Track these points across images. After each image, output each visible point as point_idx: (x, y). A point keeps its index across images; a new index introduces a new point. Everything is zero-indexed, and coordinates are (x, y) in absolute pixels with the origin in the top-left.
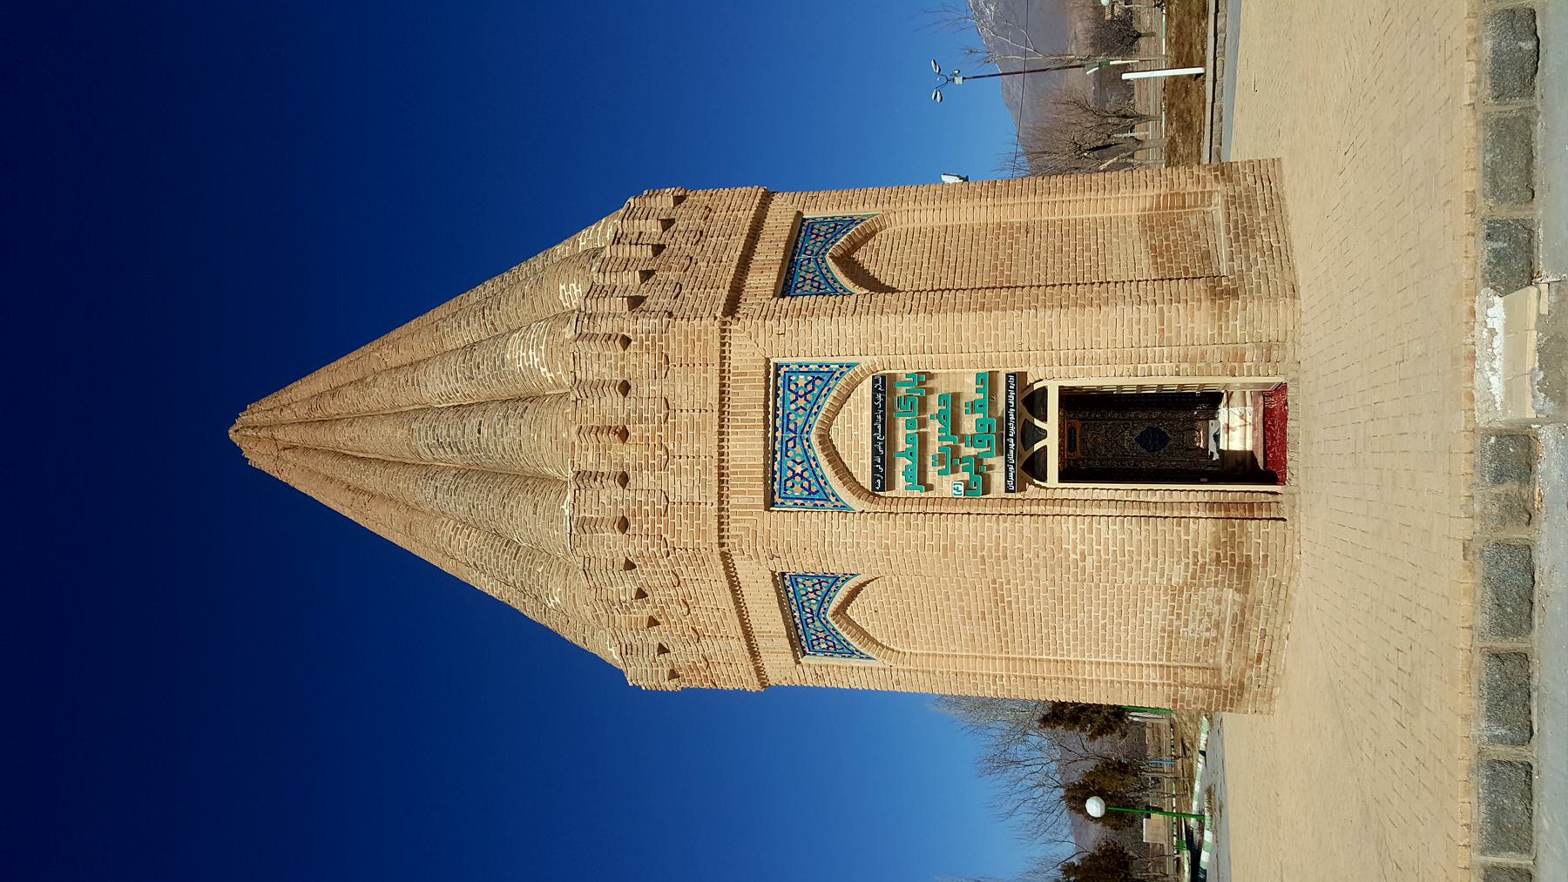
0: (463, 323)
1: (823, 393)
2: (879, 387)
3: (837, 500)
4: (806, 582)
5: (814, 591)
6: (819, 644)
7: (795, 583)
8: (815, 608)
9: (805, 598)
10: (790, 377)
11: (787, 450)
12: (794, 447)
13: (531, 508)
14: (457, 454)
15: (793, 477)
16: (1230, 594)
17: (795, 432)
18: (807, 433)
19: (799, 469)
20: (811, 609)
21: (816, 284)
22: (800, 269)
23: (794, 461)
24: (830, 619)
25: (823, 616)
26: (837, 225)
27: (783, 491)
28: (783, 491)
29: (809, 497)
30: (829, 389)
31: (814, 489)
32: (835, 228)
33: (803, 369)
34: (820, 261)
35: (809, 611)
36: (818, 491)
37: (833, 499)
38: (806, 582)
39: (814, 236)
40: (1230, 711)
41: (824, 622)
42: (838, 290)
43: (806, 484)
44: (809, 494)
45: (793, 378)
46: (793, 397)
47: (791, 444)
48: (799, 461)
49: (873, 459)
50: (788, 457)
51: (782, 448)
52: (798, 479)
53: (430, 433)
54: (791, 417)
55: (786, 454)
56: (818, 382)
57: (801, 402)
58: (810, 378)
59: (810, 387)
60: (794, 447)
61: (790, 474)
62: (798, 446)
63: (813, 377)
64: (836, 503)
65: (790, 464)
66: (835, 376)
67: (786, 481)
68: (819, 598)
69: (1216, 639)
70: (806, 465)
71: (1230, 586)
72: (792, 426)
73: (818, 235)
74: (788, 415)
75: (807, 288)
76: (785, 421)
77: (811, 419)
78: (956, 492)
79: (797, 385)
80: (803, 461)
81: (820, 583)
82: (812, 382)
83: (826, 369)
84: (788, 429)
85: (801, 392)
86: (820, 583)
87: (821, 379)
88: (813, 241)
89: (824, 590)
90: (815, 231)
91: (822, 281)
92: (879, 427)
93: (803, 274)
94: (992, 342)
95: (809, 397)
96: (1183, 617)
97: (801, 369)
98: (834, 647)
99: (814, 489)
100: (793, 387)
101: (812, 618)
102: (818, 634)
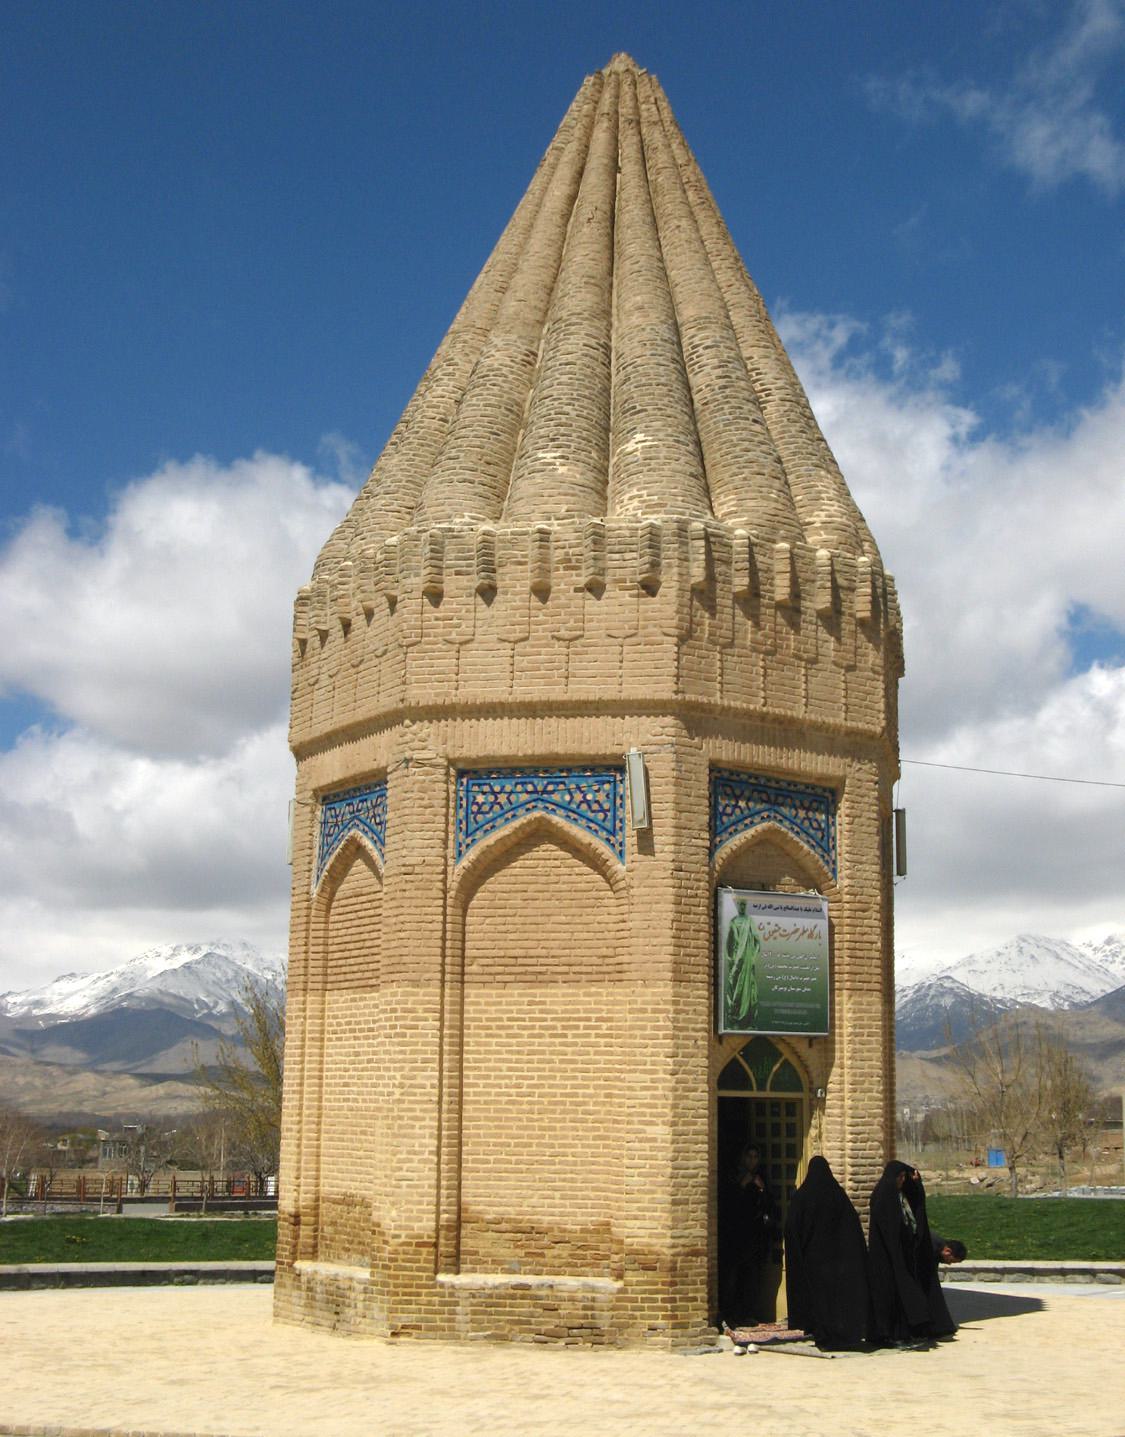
11: (760, 792)
31: (725, 819)
36: (723, 823)
45: (823, 807)
50: (753, 791)
56: (820, 835)
58: (823, 825)
59: (815, 824)
77: (787, 823)
82: (819, 828)
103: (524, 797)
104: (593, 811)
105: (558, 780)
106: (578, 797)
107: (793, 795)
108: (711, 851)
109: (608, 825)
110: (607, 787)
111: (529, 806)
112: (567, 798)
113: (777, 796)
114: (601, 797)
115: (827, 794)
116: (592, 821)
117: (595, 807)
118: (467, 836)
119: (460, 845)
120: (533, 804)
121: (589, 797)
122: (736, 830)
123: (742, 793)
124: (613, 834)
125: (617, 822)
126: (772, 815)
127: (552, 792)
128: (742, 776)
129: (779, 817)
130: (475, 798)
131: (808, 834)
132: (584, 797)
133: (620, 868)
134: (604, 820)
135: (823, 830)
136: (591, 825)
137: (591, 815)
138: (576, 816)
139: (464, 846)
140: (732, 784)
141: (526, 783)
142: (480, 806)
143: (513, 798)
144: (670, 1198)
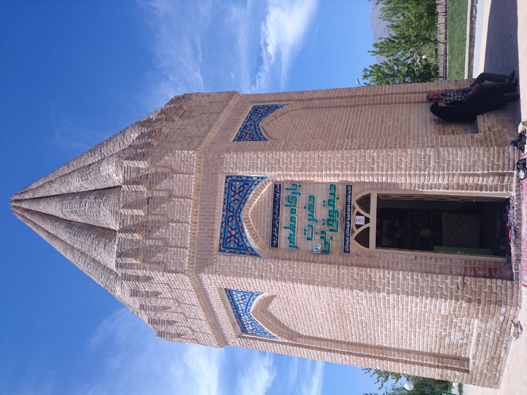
0: (93, 154)
2: (277, 190)
3: (252, 251)
4: (237, 294)
5: (242, 300)
6: (248, 327)
8: (244, 308)
9: (238, 303)
10: (232, 183)
11: (228, 222)
12: (232, 220)
13: (103, 246)
14: (78, 217)
16: (476, 322)
17: (233, 213)
18: (239, 213)
19: (233, 233)
20: (242, 309)
21: (252, 136)
22: (246, 129)
23: (231, 228)
24: (252, 315)
25: (248, 313)
26: (269, 109)
27: (225, 244)
28: (225, 244)
29: (238, 248)
30: (252, 190)
31: (240, 244)
32: (267, 110)
34: (256, 125)
35: (241, 309)
36: (242, 245)
37: (250, 250)
38: (237, 294)
39: (257, 114)
40: (474, 384)
41: (249, 316)
42: (262, 139)
43: (237, 241)
44: (238, 246)
45: (234, 184)
46: (233, 194)
47: (230, 219)
48: (234, 228)
49: (272, 229)
50: (228, 225)
51: (226, 221)
52: (233, 238)
53: (69, 206)
54: (232, 204)
56: (246, 186)
57: (237, 196)
58: (242, 184)
59: (242, 189)
60: (232, 220)
61: (229, 235)
62: (234, 221)
63: (244, 183)
64: (253, 253)
65: (229, 229)
66: (255, 183)
67: (227, 238)
68: (245, 303)
69: (466, 344)
70: (237, 231)
71: (477, 317)
72: (231, 209)
73: (258, 113)
75: (247, 138)
76: (228, 206)
78: (316, 250)
79: (235, 187)
81: (244, 295)
82: (243, 186)
84: (230, 211)
85: (237, 191)
86: (244, 295)
87: (247, 184)
88: (255, 116)
89: (247, 299)
90: (258, 112)
91: (255, 135)
92: (277, 212)
93: (246, 131)
94: (340, 167)
95: (241, 194)
96: (448, 331)
97: (238, 179)
98: (256, 329)
99: (240, 244)
100: (233, 188)
101: (243, 313)
102: (247, 322)
106: (241, 302)
107: (230, 201)
108: (254, 254)
113: (230, 211)
115: (228, 180)
123: (229, 232)
126: (238, 215)
128: (222, 232)
133: (266, 294)
135: (244, 184)
140: (226, 237)
144: (429, 298)
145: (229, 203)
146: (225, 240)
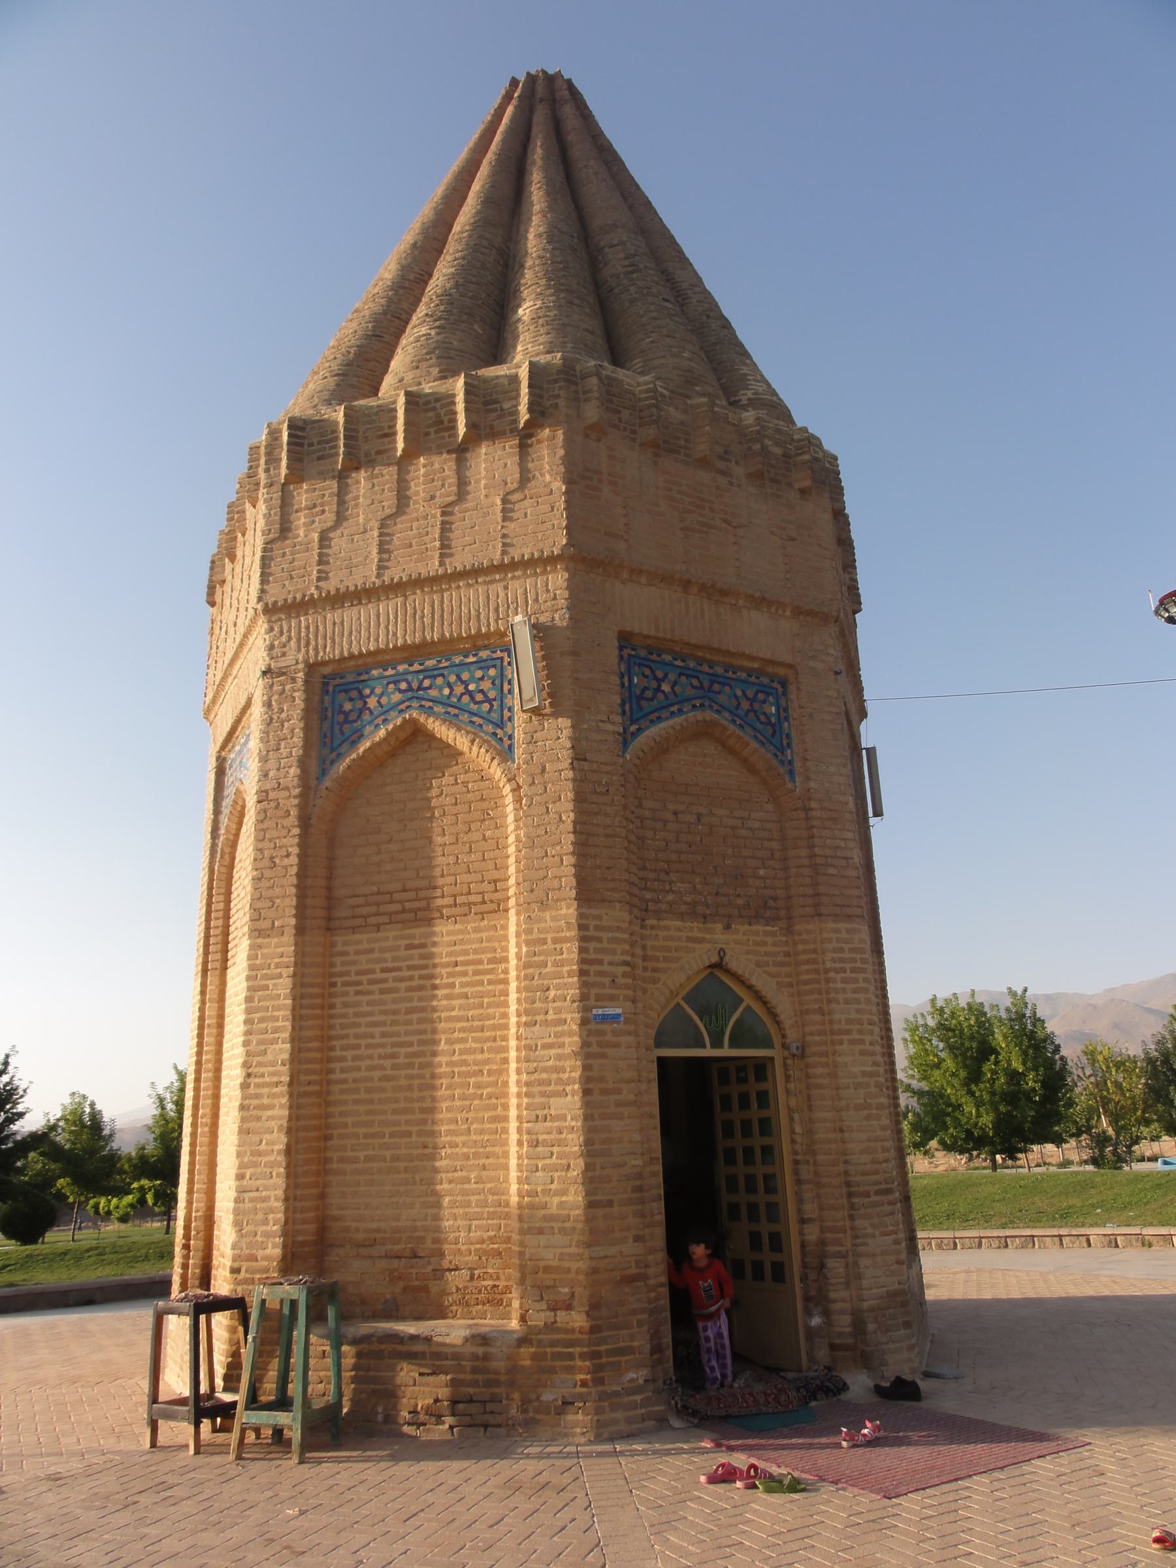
1: (758, 735)
7: (483, 665)
11: (688, 676)
12: (693, 687)
15: (656, 678)
17: (710, 690)
18: (711, 707)
19: (666, 687)
23: (675, 683)
27: (637, 661)
28: (637, 661)
31: (643, 703)
33: (784, 713)
36: (641, 709)
37: (633, 728)
43: (649, 694)
45: (771, 698)
50: (680, 675)
52: (654, 684)
54: (727, 688)
55: (683, 674)
56: (769, 730)
57: (745, 705)
58: (773, 720)
59: (763, 718)
60: (693, 687)
61: (660, 674)
62: (693, 692)
66: (778, 753)
74: (728, 685)
77: (727, 714)
80: (676, 695)
82: (769, 723)
83: (785, 742)
84: (712, 682)
87: (774, 734)
103: (397, 697)
104: (476, 703)
105: (435, 673)
106: (459, 689)
107: (732, 683)
109: (495, 716)
110: (492, 672)
111: (403, 707)
112: (446, 691)
113: (712, 682)
114: (486, 685)
115: (775, 685)
116: (475, 715)
117: (479, 697)
118: (332, 750)
119: (324, 762)
120: (407, 704)
121: (472, 687)
122: (659, 718)
123: (666, 675)
124: (501, 725)
125: (506, 711)
126: (707, 703)
127: (430, 688)
129: (716, 707)
130: (341, 706)
131: (754, 728)
132: (466, 688)
134: (489, 712)
135: (773, 726)
136: (475, 719)
137: (473, 707)
138: (456, 711)
139: (328, 762)
140: (651, 664)
141: (399, 681)
142: (346, 714)
143: (384, 700)
145: (727, 681)
146: (646, 663)
